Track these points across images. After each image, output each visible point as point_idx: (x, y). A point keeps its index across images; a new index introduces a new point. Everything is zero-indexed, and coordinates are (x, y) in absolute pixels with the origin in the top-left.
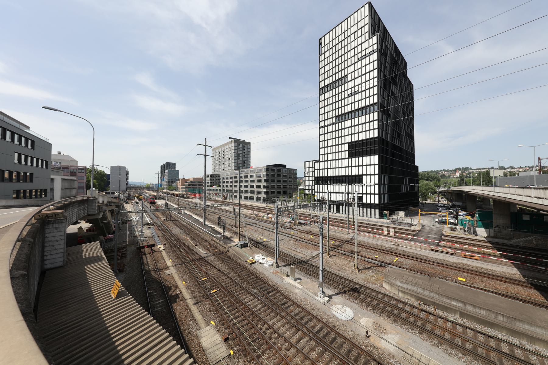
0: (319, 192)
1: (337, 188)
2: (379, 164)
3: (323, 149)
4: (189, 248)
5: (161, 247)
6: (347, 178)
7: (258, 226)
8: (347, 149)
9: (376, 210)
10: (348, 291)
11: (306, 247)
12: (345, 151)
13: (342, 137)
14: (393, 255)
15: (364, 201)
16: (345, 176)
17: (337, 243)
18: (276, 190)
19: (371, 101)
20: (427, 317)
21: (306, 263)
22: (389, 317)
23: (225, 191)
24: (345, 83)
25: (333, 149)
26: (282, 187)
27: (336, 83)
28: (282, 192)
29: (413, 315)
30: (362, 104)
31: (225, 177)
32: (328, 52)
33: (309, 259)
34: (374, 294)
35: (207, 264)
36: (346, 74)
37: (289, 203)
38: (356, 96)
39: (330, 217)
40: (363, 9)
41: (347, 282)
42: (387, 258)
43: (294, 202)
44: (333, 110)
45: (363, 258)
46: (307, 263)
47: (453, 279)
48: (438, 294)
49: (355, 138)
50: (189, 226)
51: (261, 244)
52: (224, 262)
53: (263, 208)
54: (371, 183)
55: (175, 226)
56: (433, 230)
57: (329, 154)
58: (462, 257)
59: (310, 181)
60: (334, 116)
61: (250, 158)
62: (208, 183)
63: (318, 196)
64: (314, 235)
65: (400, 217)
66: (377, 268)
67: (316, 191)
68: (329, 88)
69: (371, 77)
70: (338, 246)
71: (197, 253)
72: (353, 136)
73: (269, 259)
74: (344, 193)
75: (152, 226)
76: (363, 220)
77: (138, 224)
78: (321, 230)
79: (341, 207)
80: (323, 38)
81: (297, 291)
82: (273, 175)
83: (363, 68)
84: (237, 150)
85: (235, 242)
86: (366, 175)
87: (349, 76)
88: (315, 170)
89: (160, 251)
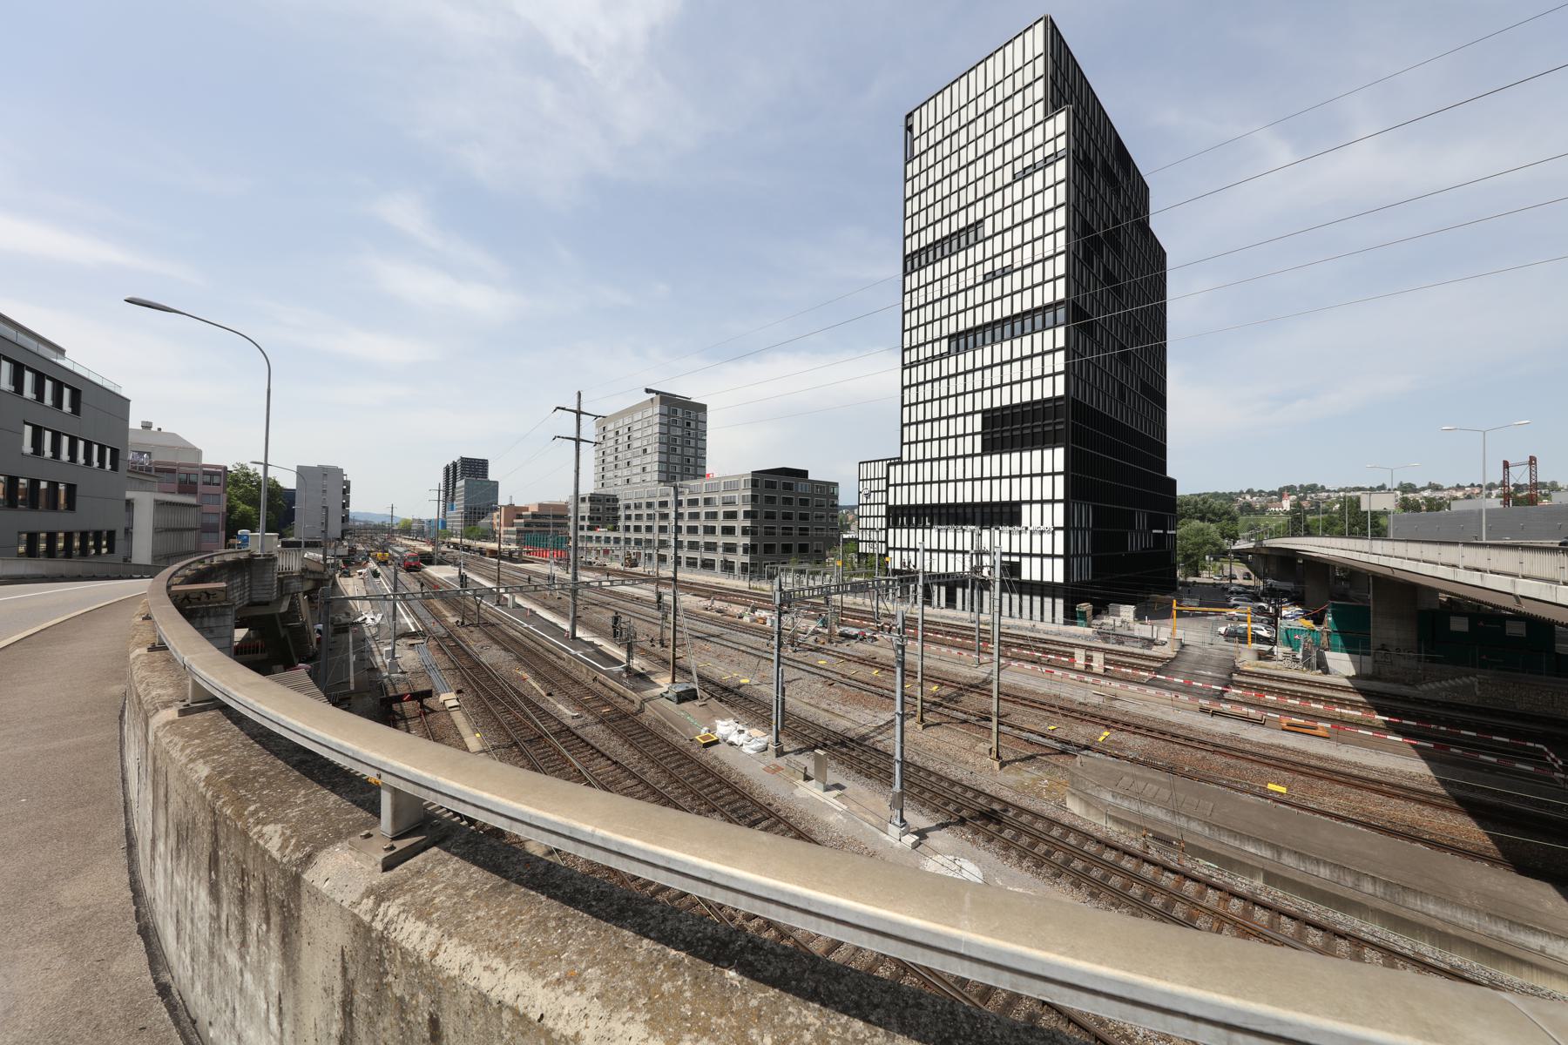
0: (898, 549)
1: (949, 537)
2: (1065, 473)
3: (913, 427)
4: (528, 702)
5: (448, 698)
6: (978, 510)
7: (725, 643)
8: (978, 428)
9: (1057, 600)
10: (972, 818)
11: (857, 701)
12: (973, 434)
13: (965, 393)
14: (1097, 723)
15: (1025, 576)
16: (973, 505)
17: (946, 691)
18: (778, 542)
19: (1047, 295)
20: (1179, 885)
21: (857, 743)
22: (1078, 887)
23: (633, 543)
24: (977, 242)
25: (941, 429)
26: (795, 532)
27: (951, 241)
28: (795, 548)
29: (1142, 880)
30: (1023, 303)
31: (632, 503)
32: (931, 152)
33: (867, 734)
34: (1039, 825)
35: (582, 747)
36: (980, 216)
37: (813, 579)
38: (1007, 279)
39: (925, 618)
40: (1029, 34)
41: (969, 795)
42: (1081, 732)
43: (828, 576)
44: (941, 319)
45: (1017, 732)
46: (861, 745)
47: (1255, 787)
48: (1210, 826)
49: (1002, 398)
50: (528, 641)
51: (732, 691)
52: (629, 740)
53: (740, 591)
54: (1045, 525)
55: (487, 642)
56: (1210, 658)
57: (928, 440)
58: (1283, 730)
59: (874, 517)
60: (945, 333)
62: (583, 518)
63: (895, 560)
64: (883, 669)
65: (1123, 622)
66: (1053, 759)
67: (891, 544)
68: (931, 254)
69: (1049, 229)
70: (949, 699)
71: (552, 717)
72: (997, 392)
73: (756, 732)
74: (968, 552)
75: (422, 641)
76: (1020, 628)
77: (382, 635)
78: (900, 652)
79: (959, 591)
80: (917, 114)
81: (831, 818)
82: (770, 500)
83: (1028, 203)
84: (668, 425)
85: (660, 686)
86: (1031, 502)
87: (988, 222)
88: (888, 485)
89: (447, 711)
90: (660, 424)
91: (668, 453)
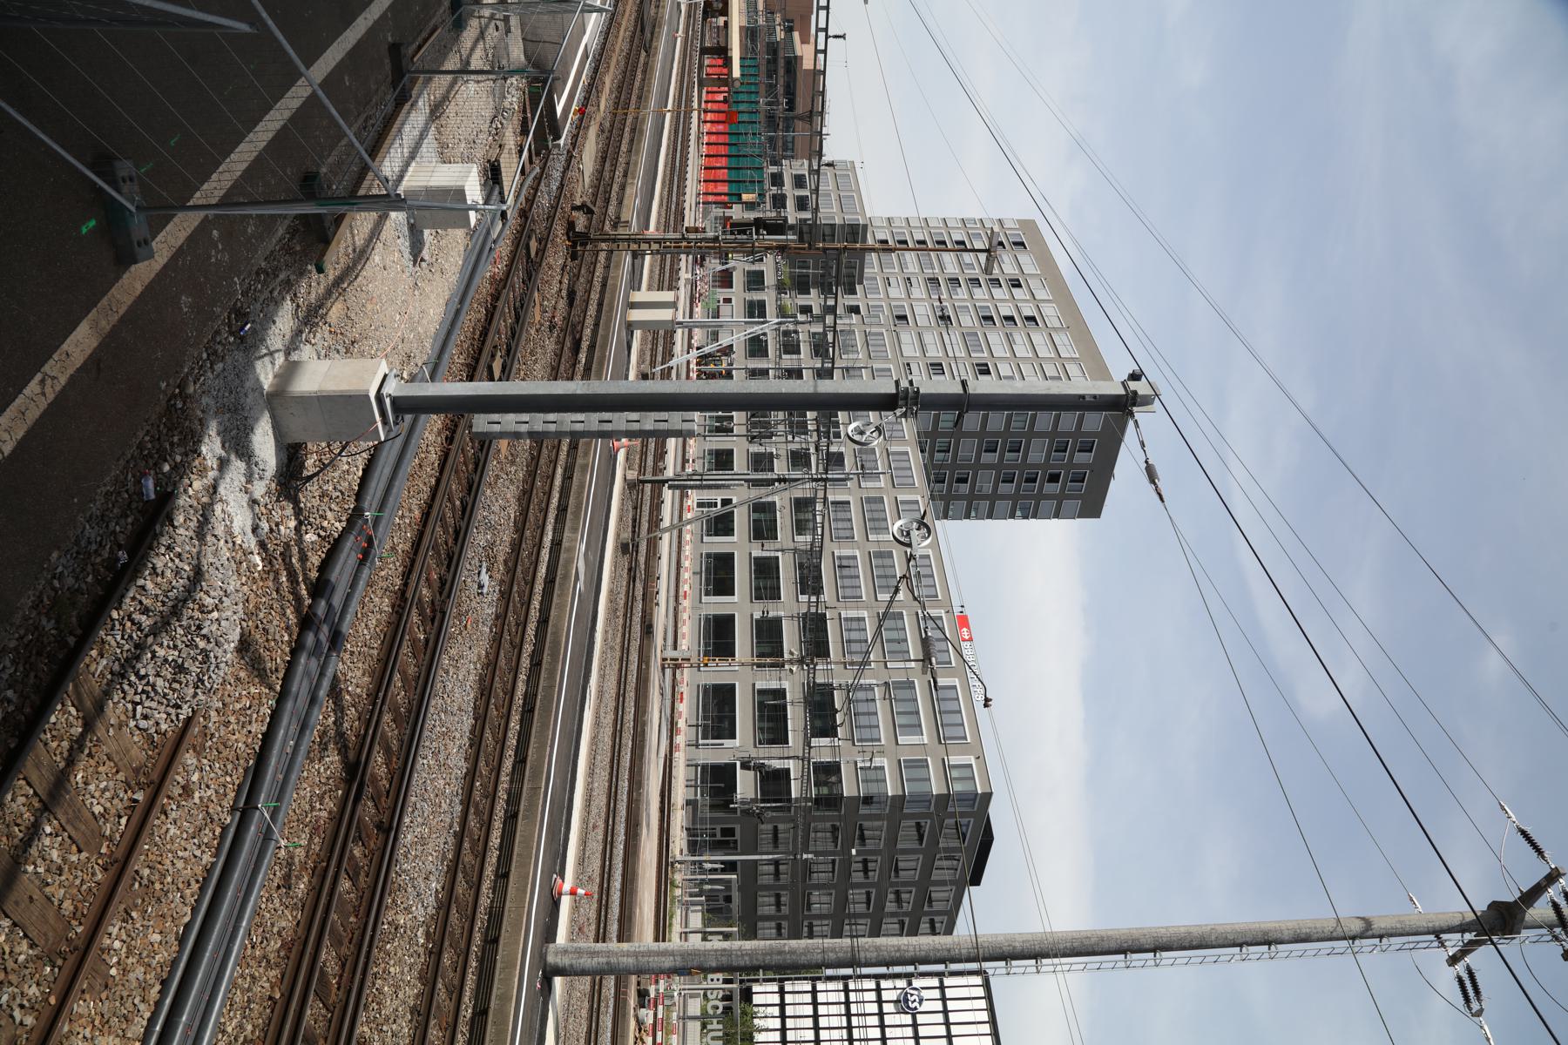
61: (990, 516)
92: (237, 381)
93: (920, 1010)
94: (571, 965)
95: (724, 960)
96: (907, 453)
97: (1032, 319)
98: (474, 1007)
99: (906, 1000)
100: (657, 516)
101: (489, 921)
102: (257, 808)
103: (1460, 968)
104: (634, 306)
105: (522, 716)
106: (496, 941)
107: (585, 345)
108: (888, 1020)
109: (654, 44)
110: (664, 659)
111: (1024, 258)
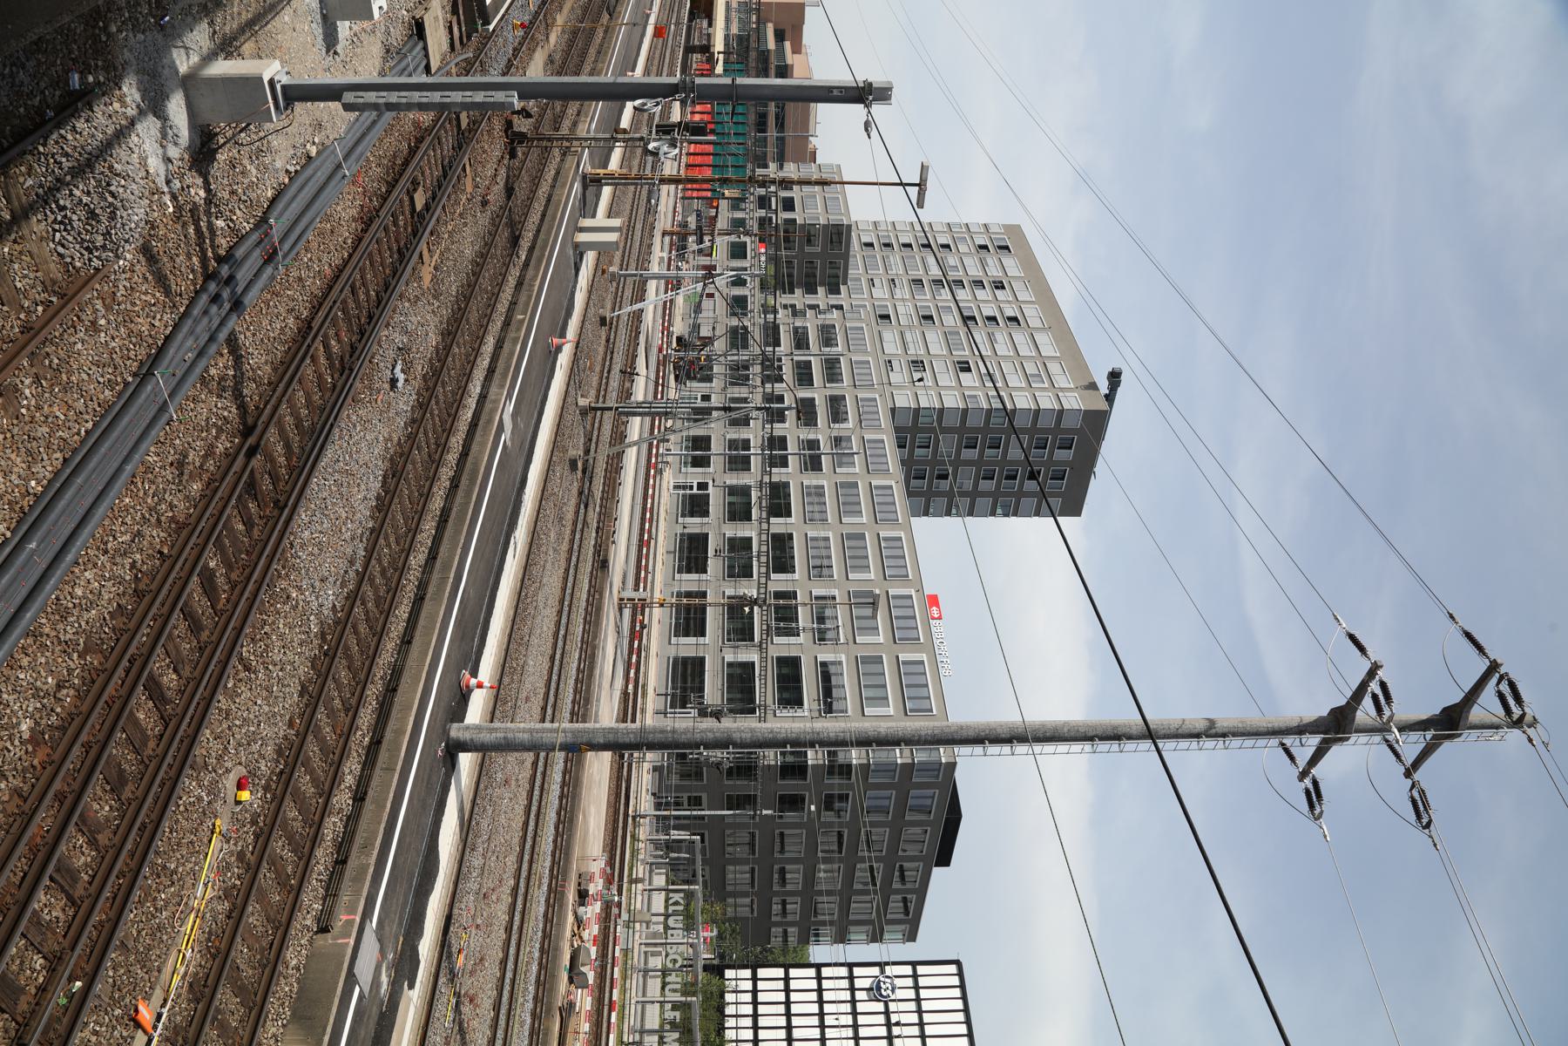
62: (789, 205)
90: (1037, 412)
91: (962, 429)
92: (155, 55)
93: (893, 997)
94: (472, 740)
95: (611, 737)
96: (883, 441)
97: (1014, 319)
98: (372, 738)
99: (879, 988)
100: (617, 464)
101: (392, 675)
102: (154, 375)
103: (1308, 782)
104: (582, 230)
105: (439, 525)
106: (395, 690)
107: (525, 244)
108: (860, 1007)
109: (618, 9)
110: (622, 599)
111: (1010, 262)
